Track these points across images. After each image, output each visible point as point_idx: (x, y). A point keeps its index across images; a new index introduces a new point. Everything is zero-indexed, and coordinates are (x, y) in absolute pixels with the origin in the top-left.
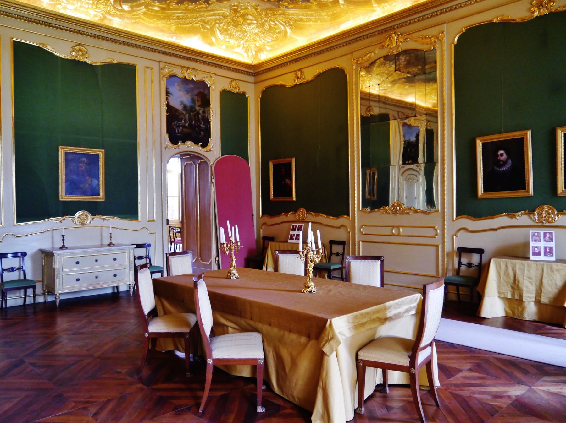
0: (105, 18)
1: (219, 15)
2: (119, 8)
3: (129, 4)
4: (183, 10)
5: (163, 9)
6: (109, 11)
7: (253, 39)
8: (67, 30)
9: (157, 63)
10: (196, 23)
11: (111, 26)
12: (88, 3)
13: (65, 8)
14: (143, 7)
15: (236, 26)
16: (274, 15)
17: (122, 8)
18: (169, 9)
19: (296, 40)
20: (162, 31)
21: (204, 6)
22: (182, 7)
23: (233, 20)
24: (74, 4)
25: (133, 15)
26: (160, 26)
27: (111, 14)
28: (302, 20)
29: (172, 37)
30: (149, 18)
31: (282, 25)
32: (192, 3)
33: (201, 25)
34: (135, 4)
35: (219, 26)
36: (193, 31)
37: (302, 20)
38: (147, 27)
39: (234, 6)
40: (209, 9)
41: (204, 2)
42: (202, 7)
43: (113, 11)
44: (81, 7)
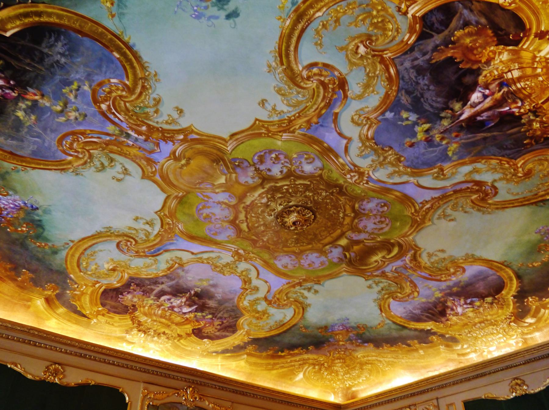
2: (526, 325)
3: (529, 316)
11: (537, 343)
12: (500, 338)
14: (543, 310)
17: (527, 323)
27: (527, 334)
43: (525, 330)
44: (499, 343)
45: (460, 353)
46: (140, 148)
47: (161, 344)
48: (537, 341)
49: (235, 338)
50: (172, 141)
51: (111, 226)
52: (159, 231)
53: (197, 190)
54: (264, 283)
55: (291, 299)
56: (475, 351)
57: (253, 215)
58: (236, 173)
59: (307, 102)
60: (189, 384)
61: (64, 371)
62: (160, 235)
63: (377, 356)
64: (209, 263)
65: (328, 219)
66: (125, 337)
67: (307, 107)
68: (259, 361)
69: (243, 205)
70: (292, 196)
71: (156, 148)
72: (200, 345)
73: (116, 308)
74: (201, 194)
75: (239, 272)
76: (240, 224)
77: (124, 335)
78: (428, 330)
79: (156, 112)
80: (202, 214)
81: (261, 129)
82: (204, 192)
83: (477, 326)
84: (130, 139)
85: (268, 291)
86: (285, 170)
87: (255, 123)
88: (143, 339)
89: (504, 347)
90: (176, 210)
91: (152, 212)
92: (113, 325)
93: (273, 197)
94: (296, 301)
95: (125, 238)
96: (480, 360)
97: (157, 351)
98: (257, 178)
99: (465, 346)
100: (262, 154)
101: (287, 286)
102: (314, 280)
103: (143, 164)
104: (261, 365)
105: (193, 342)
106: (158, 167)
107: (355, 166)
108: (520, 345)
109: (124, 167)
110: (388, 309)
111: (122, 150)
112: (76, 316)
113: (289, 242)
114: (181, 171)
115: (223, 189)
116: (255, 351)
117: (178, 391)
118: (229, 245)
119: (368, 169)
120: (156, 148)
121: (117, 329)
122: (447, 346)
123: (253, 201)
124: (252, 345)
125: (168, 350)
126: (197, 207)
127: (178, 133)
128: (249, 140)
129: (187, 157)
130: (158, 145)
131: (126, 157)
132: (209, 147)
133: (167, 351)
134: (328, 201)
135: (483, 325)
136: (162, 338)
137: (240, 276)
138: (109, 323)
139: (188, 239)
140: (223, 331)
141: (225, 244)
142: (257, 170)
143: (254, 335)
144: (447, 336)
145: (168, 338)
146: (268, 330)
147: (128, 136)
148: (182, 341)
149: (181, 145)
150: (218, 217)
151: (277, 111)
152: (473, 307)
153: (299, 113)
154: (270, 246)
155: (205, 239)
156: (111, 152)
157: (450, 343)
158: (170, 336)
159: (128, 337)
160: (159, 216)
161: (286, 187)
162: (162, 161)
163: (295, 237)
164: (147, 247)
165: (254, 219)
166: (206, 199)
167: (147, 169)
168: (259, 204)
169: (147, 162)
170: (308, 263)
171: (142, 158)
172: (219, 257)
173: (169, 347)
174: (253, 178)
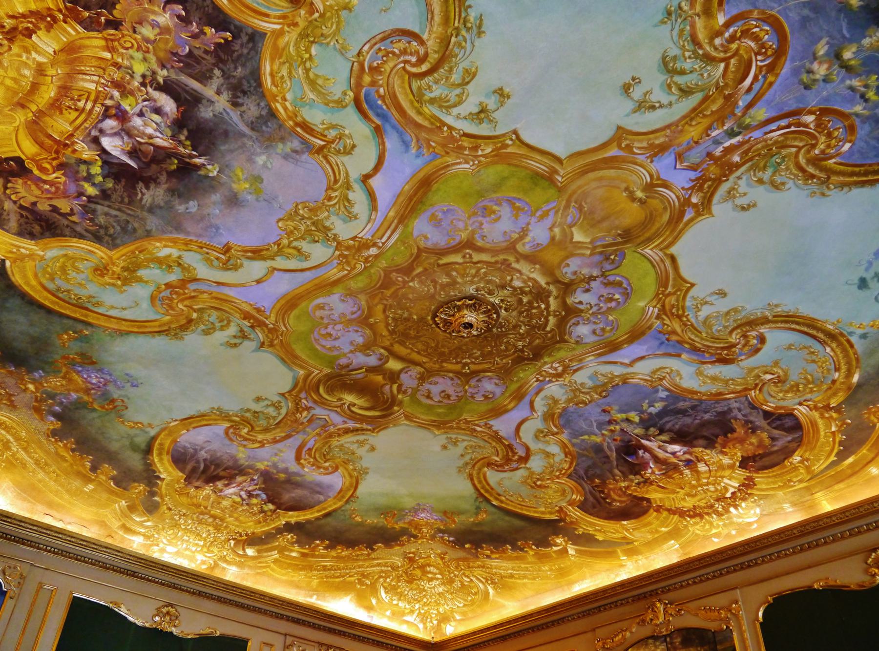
0: (216, 565)
1: (386, 565)
2: (241, 553)
3: (257, 548)
4: (333, 557)
5: (304, 555)
6: (225, 556)
7: (436, 602)
8: (157, 583)
9: (282, 637)
10: (350, 576)
12: (197, 544)
13: (163, 551)
15: (410, 581)
16: (469, 567)
18: (314, 556)
19: (503, 606)
20: (297, 586)
21: (366, 552)
22: (333, 553)
23: (406, 573)
24: (177, 545)
25: (260, 563)
26: (295, 579)
27: (226, 561)
28: (512, 576)
29: (311, 596)
30: (281, 567)
31: (481, 582)
32: (348, 548)
33: (358, 579)
34: (265, 547)
35: (385, 581)
36: (343, 588)
37: (512, 576)
38: (277, 580)
39: (409, 553)
40: (373, 556)
41: (367, 548)
42: (362, 554)
43: (230, 557)
44: (187, 549)
45: (128, 525)
46: (696, 143)
48: (225, 575)
50: (692, 188)
51: (485, 38)
52: (450, 128)
53: (564, 203)
56: (147, 537)
57: (483, 270)
58: (591, 255)
59: (707, 333)
62: (439, 128)
63: (18, 439)
64: (330, 199)
65: (460, 348)
67: (700, 333)
69: (511, 259)
70: (521, 313)
71: (685, 164)
74: (554, 208)
78: (159, 478)
79: (760, 181)
80: (499, 205)
81: (673, 288)
82: (557, 212)
83: (201, 516)
84: (723, 134)
86: (581, 307)
87: (687, 282)
89: (185, 557)
90: (516, 166)
93: (523, 292)
95: (434, 57)
96: (141, 551)
98: (574, 277)
99: (149, 524)
100: (625, 285)
103: (656, 138)
106: (641, 159)
107: (575, 371)
108: (204, 567)
109: (661, 106)
110: (195, 425)
111: (705, 116)
113: (400, 312)
114: (619, 188)
115: (557, 238)
118: (396, 236)
119: (567, 380)
120: (685, 164)
122: (132, 508)
123: (519, 272)
126: (519, 199)
127: (704, 198)
128: (657, 273)
129: (648, 200)
130: (693, 168)
131: (684, 117)
132: (659, 229)
134: (503, 348)
135: (211, 520)
139: (421, 175)
141: (399, 231)
142: (592, 278)
144: (157, 499)
147: (731, 134)
149: (677, 197)
150: (486, 226)
151: (702, 305)
152: (243, 500)
153: (692, 325)
155: (420, 201)
156: (706, 99)
157: (141, 508)
160: (504, 135)
161: (543, 306)
162: (653, 167)
163: (415, 317)
164: (394, 97)
165: (473, 271)
166: (539, 214)
167: (639, 141)
168: (509, 278)
169: (659, 145)
171: (670, 141)
174: (575, 273)
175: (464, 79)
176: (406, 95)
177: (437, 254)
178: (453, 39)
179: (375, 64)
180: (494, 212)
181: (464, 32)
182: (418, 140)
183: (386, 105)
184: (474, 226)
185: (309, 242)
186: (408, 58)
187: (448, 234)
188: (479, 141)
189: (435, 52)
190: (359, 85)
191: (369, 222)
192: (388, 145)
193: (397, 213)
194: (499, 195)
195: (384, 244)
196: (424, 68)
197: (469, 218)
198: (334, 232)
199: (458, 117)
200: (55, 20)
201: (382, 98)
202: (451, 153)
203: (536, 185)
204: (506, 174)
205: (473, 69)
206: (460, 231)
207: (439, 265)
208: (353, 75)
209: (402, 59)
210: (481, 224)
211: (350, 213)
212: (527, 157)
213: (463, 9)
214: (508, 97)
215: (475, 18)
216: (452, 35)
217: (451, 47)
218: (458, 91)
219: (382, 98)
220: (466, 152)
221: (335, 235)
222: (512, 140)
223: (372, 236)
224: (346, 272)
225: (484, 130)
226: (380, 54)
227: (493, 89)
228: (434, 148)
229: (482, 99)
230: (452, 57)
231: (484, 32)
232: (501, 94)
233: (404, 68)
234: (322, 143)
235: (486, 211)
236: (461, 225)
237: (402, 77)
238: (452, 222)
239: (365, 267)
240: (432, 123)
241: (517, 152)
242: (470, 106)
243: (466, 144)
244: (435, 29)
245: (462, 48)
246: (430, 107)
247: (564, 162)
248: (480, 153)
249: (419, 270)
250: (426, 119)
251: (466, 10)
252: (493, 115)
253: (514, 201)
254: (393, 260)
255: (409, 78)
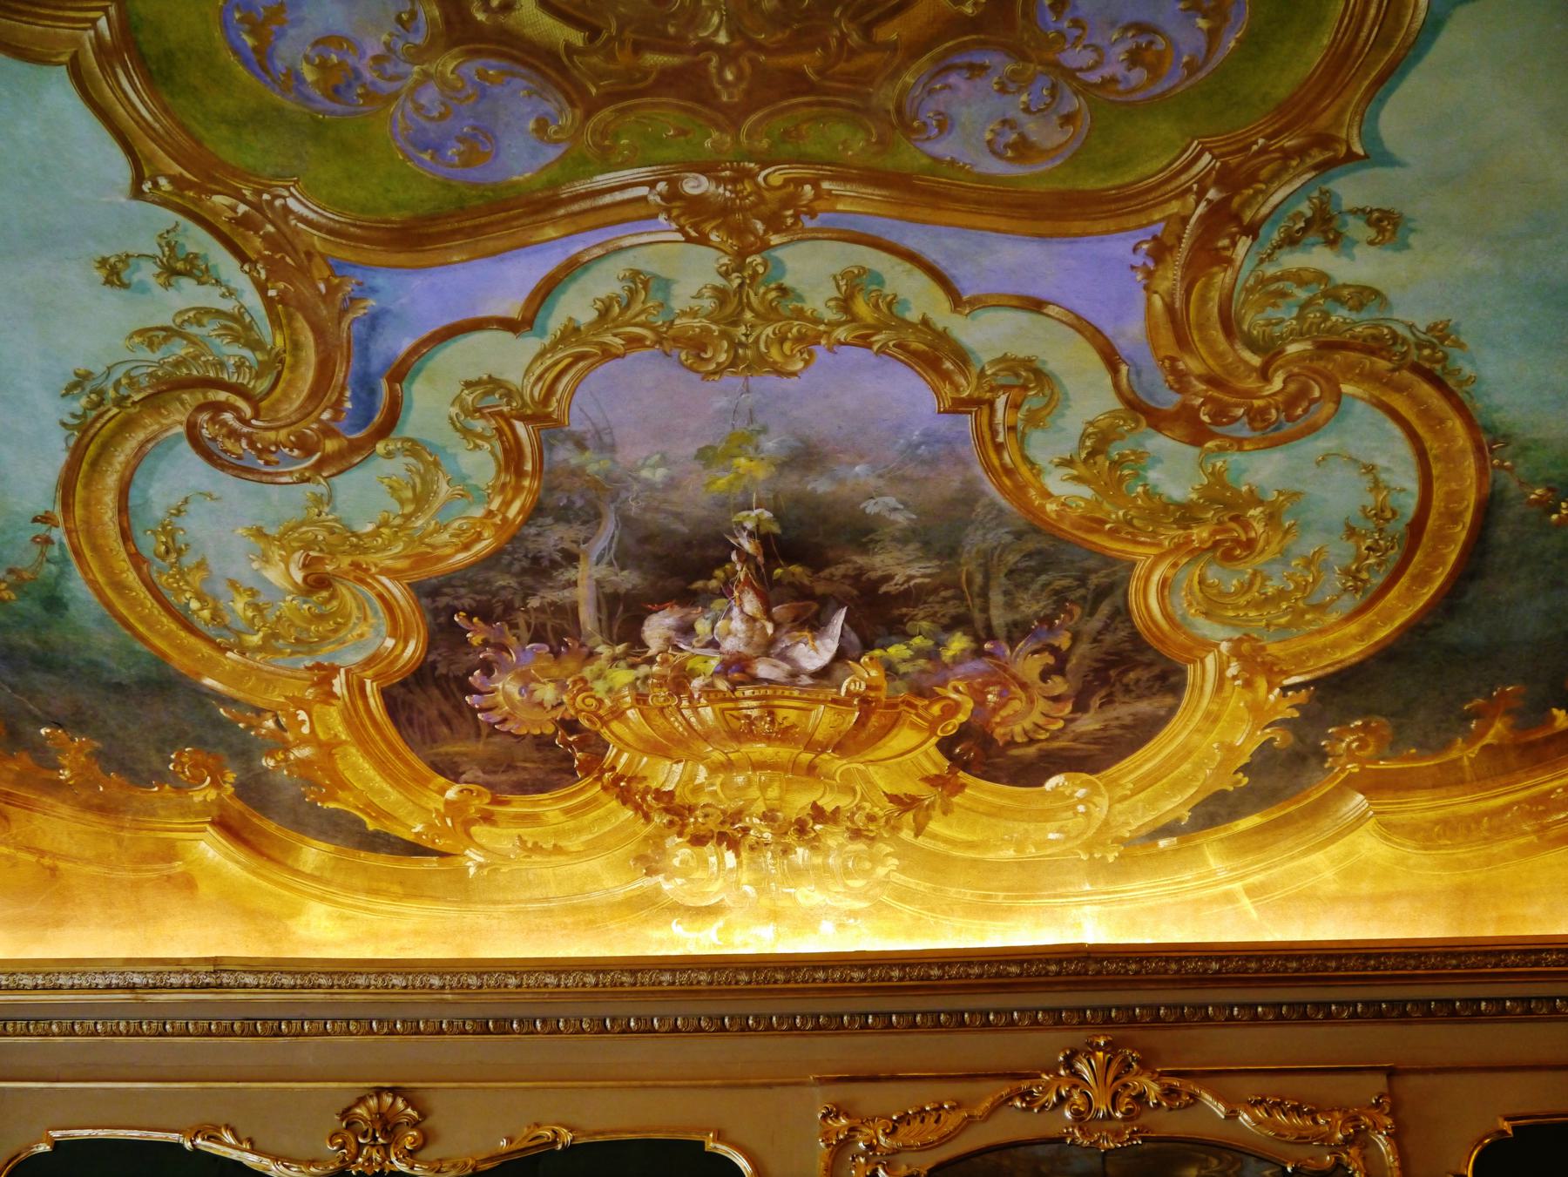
47: (847, 873)
49: (1212, 718)
51: (81, 365)
52: (262, 288)
54: (1024, 318)
55: (1292, 349)
60: (1079, 1037)
61: (423, 1115)
62: (283, 298)
66: (658, 891)
68: (1463, 804)
72: (1046, 816)
73: (511, 767)
75: (830, 315)
76: (510, 21)
77: (648, 882)
85: (1111, 359)
88: (745, 876)
91: (123, 200)
92: (558, 850)
94: (1327, 347)
95: (191, 398)
97: (853, 914)
101: (1170, 277)
102: (1287, 155)
104: (1496, 825)
105: (996, 813)
112: (380, 861)
116: (1393, 747)
117: (1025, 1085)
121: (595, 864)
124: (1342, 722)
125: (905, 895)
133: (901, 899)
136: (832, 842)
137: (864, 341)
138: (537, 848)
139: (402, 258)
140: (1109, 701)
141: (581, 187)
143: (1299, 660)
145: (856, 834)
146: (1349, 602)
148: (933, 826)
150: (374, 47)
154: (787, 61)
155: (462, 210)
158: (860, 820)
159: (670, 887)
160: (165, 203)
170: (1119, 53)
172: (638, 281)
173: (898, 878)
175: (166, 339)
176: (290, 384)
177: (562, 70)
178: (137, 397)
179: (296, 452)
180: (323, 67)
181: (111, 394)
182: (344, 312)
183: (341, 394)
184: (403, 68)
185: (800, 298)
186: (237, 425)
187: (483, 94)
188: (225, 229)
189: (183, 403)
190: (354, 448)
191: (621, 249)
192: (407, 344)
193: (540, 225)
194: (278, 98)
195: (652, 185)
196: (222, 396)
197: (395, 96)
198: (720, 282)
199: (230, 293)
200: (617, 780)
201: (337, 407)
202: (301, 248)
203: (169, 55)
204: (224, 131)
205: (137, 340)
206: (444, 82)
207: (594, 33)
208: (346, 464)
209: (246, 430)
210: (377, 59)
211: (633, 293)
212: (147, 127)
213: (89, 420)
214: (103, 262)
215: (77, 398)
216: (134, 403)
217: (150, 391)
218: (193, 330)
219: (337, 407)
220: (270, 228)
221: (726, 275)
222: (156, 185)
223: (655, 216)
224: (826, 185)
225: (197, 240)
226: (273, 458)
227: (124, 292)
228: (327, 281)
229: (158, 290)
230: (158, 378)
231: (76, 374)
232: (114, 274)
233: (256, 416)
234: (520, 427)
235: (339, 84)
236: (430, 96)
237: (274, 407)
238: (442, 116)
239: (764, 166)
240: (290, 318)
241: (161, 153)
242: (189, 294)
243: (258, 242)
244: (156, 427)
245: (131, 378)
246: (268, 339)
247: (65, 58)
248: (242, 208)
249: (653, 60)
250: (293, 331)
251: (84, 415)
252: (158, 252)
253: (254, 58)
254: (682, 132)
255: (262, 400)
